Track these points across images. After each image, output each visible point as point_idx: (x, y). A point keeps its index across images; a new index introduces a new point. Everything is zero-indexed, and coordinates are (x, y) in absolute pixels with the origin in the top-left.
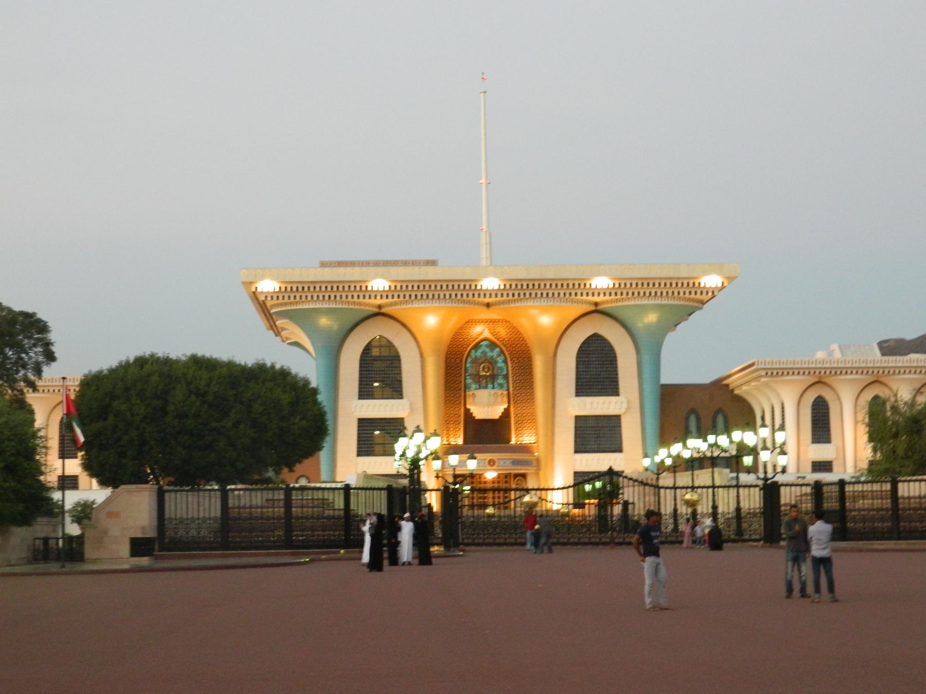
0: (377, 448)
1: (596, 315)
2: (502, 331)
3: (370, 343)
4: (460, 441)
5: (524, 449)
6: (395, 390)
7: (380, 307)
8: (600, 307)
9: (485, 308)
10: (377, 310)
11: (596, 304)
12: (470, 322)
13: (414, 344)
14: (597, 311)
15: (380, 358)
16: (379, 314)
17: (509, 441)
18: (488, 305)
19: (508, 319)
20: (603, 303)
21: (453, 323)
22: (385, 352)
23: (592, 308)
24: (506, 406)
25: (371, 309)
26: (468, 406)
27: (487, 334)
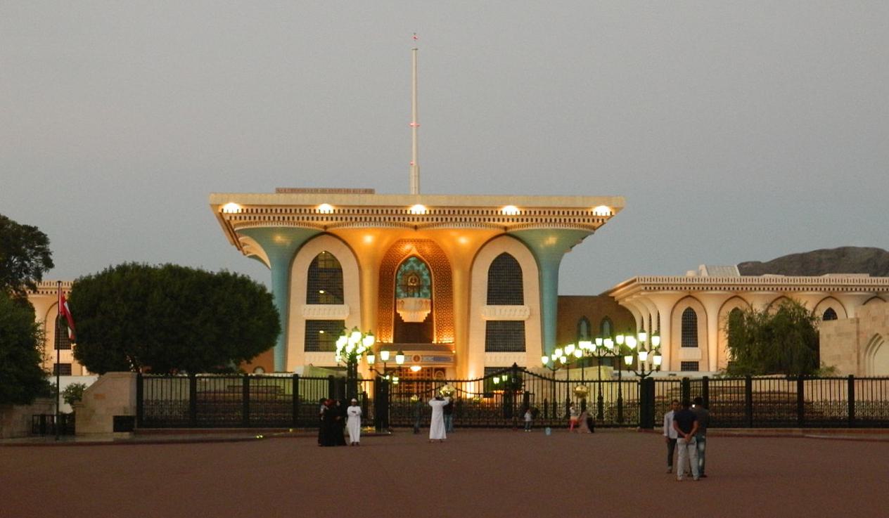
0: (321, 345)
1: (505, 237)
2: (427, 250)
3: (317, 256)
4: (391, 341)
5: (445, 347)
6: (337, 296)
7: (326, 227)
8: (509, 231)
9: (413, 230)
10: (323, 230)
11: (506, 228)
12: (402, 241)
13: (353, 258)
14: (507, 234)
15: (326, 270)
16: (325, 233)
17: (432, 340)
18: (416, 228)
19: (433, 240)
20: (511, 227)
21: (386, 242)
22: (330, 265)
23: (502, 231)
24: (429, 312)
25: (318, 229)
26: (398, 311)
27: (414, 252)
